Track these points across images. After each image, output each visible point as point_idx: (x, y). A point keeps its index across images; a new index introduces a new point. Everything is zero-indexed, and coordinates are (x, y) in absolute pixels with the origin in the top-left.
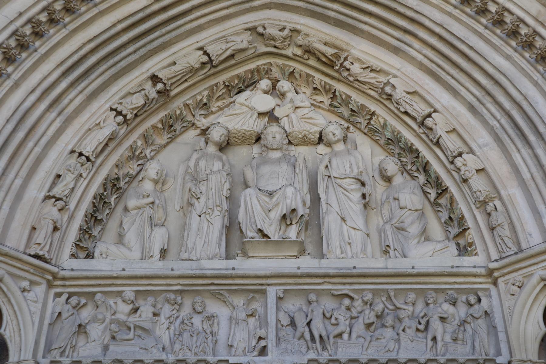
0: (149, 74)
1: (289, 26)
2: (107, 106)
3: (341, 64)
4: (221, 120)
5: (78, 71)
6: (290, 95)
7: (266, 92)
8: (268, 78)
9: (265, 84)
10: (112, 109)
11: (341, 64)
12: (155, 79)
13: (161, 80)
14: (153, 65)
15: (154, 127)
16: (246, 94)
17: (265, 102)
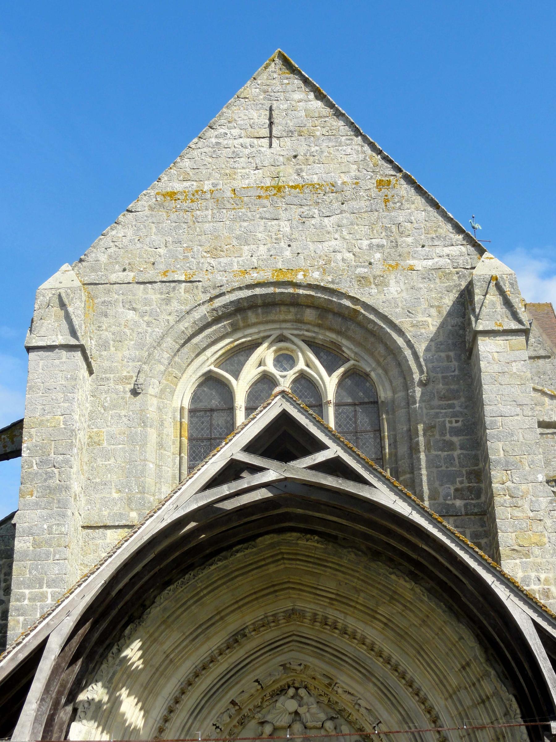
0: (230, 700)
1: (304, 663)
2: (211, 724)
3: (333, 689)
4: (269, 718)
5: (197, 711)
6: (306, 698)
7: (292, 697)
8: (294, 687)
9: (291, 691)
10: (214, 725)
11: (333, 689)
12: (233, 703)
13: (237, 704)
14: (232, 694)
15: (235, 726)
16: (282, 698)
17: (292, 705)
